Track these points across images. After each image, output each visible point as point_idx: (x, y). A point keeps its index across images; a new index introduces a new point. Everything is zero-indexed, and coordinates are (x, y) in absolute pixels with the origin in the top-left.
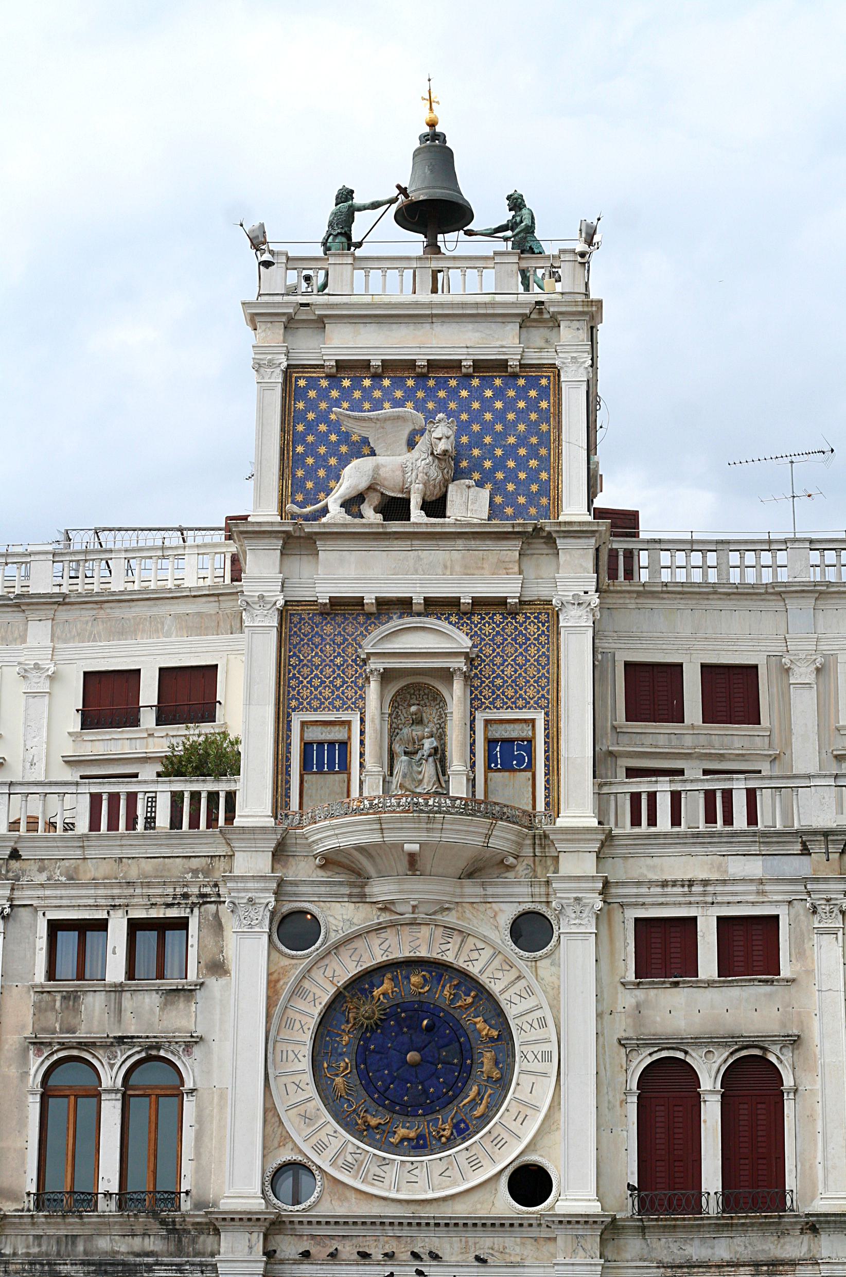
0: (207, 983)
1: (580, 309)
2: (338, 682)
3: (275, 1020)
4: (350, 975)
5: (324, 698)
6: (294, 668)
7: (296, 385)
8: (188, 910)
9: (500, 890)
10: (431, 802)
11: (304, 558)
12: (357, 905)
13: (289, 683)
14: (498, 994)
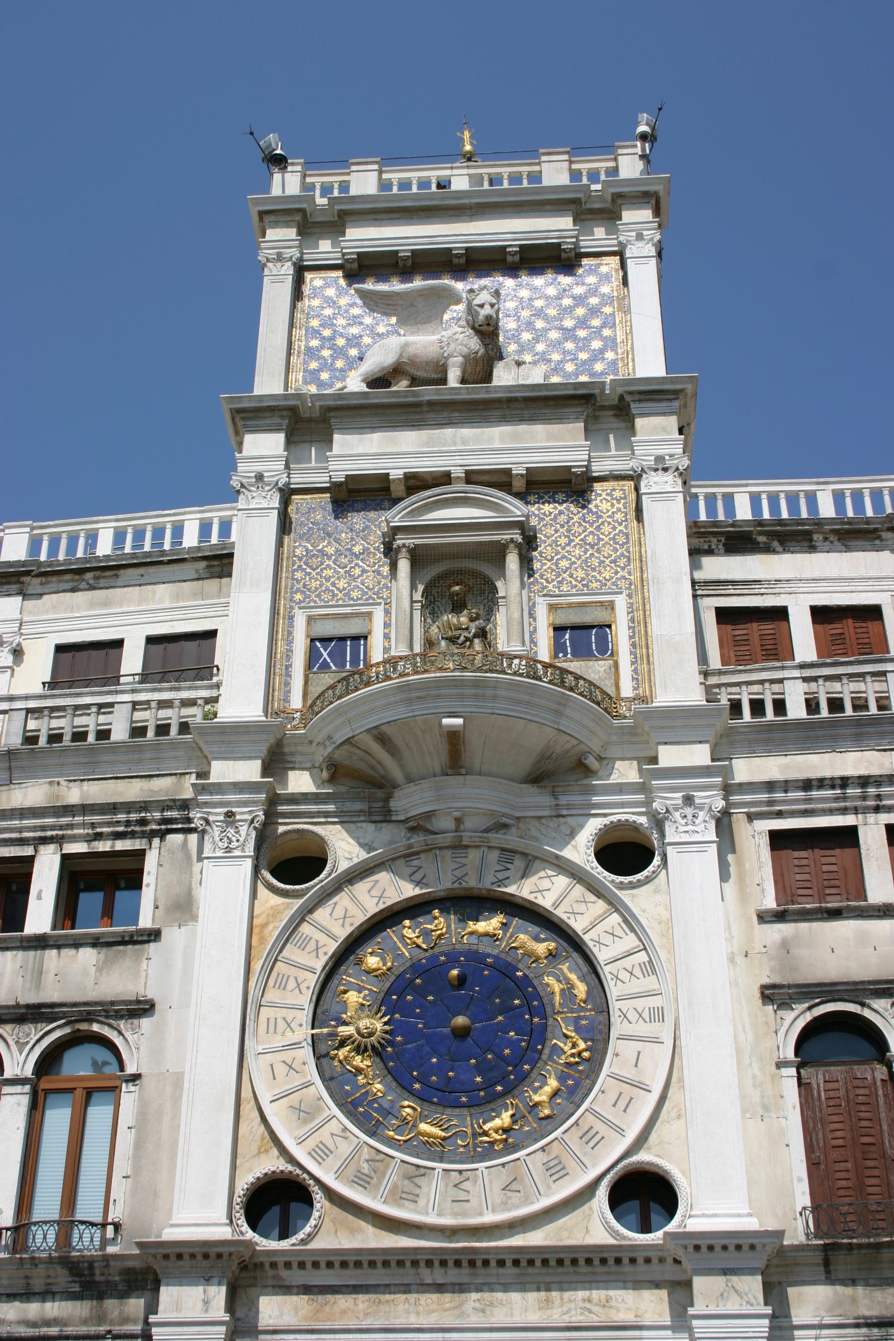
2: (357, 571)
4: (369, 915)
5: (338, 589)
6: (300, 559)
9: (576, 799)
12: (379, 825)
13: (293, 575)
14: (581, 934)
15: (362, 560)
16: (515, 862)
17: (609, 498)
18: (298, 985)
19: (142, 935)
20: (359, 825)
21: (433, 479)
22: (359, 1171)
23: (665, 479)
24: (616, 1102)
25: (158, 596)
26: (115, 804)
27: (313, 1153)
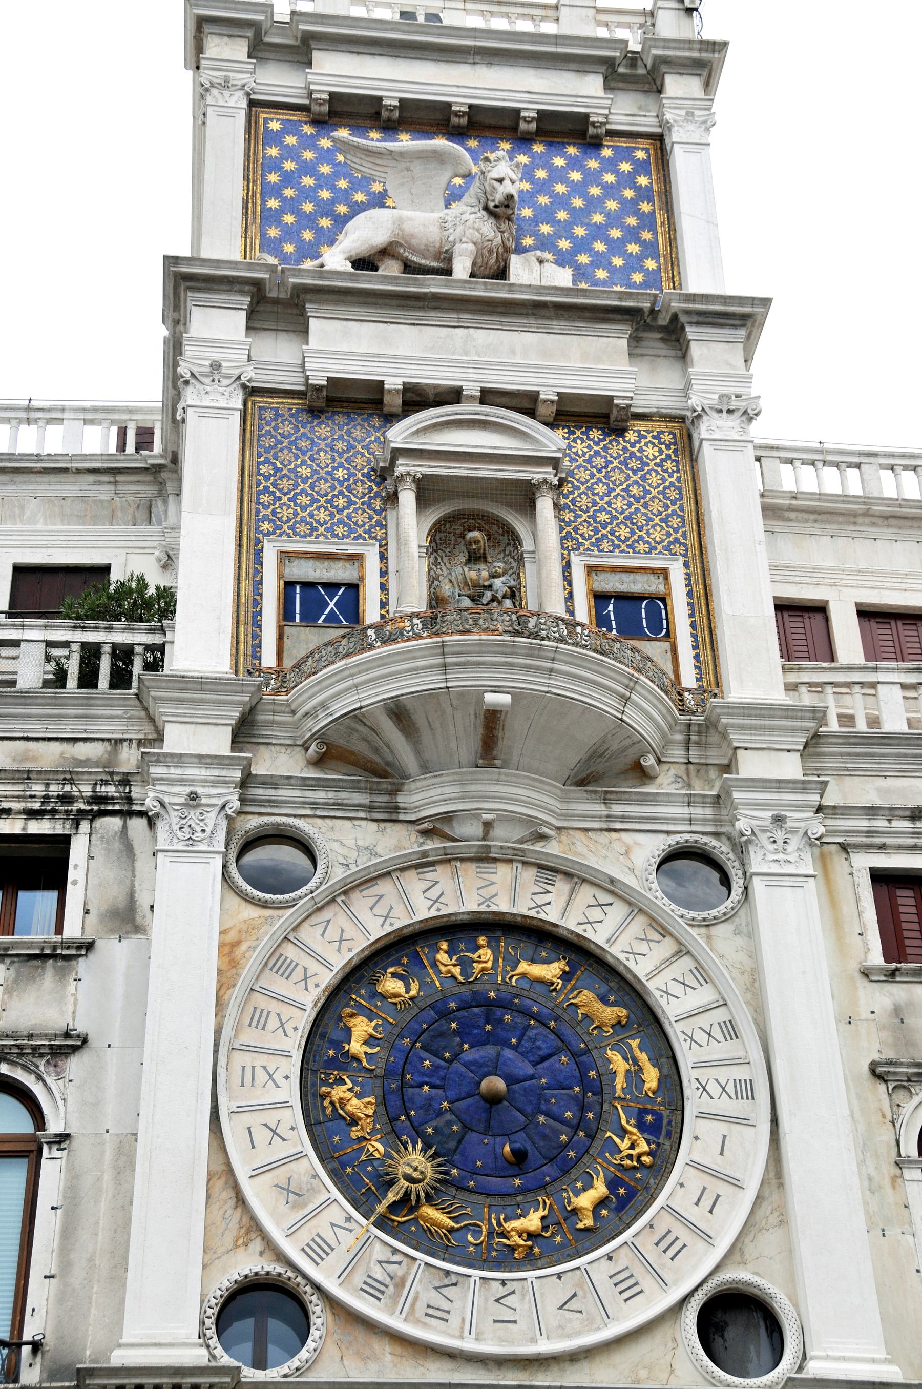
0: (99, 944)
1: (696, 55)
2: (341, 502)
3: (232, 1011)
5: (318, 522)
6: (267, 478)
7: (266, 128)
8: (69, 823)
11: (282, 336)
12: (382, 825)
13: (258, 498)
14: (644, 979)
15: (349, 489)
16: (557, 884)
17: (656, 441)
18: (282, 1025)
19: (68, 948)
20: (357, 822)
21: (437, 395)
22: (369, 1276)
23: (731, 424)
24: (699, 1200)
25: (28, 513)
26: (29, 772)
27: (307, 1249)
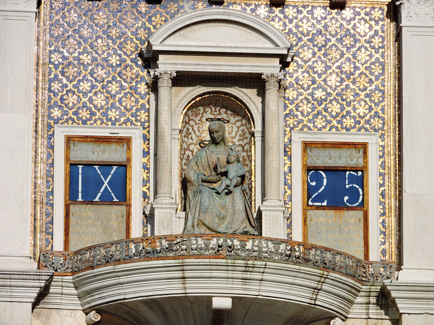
6: (56, 67)
10: (249, 245)
17: (367, 18)
